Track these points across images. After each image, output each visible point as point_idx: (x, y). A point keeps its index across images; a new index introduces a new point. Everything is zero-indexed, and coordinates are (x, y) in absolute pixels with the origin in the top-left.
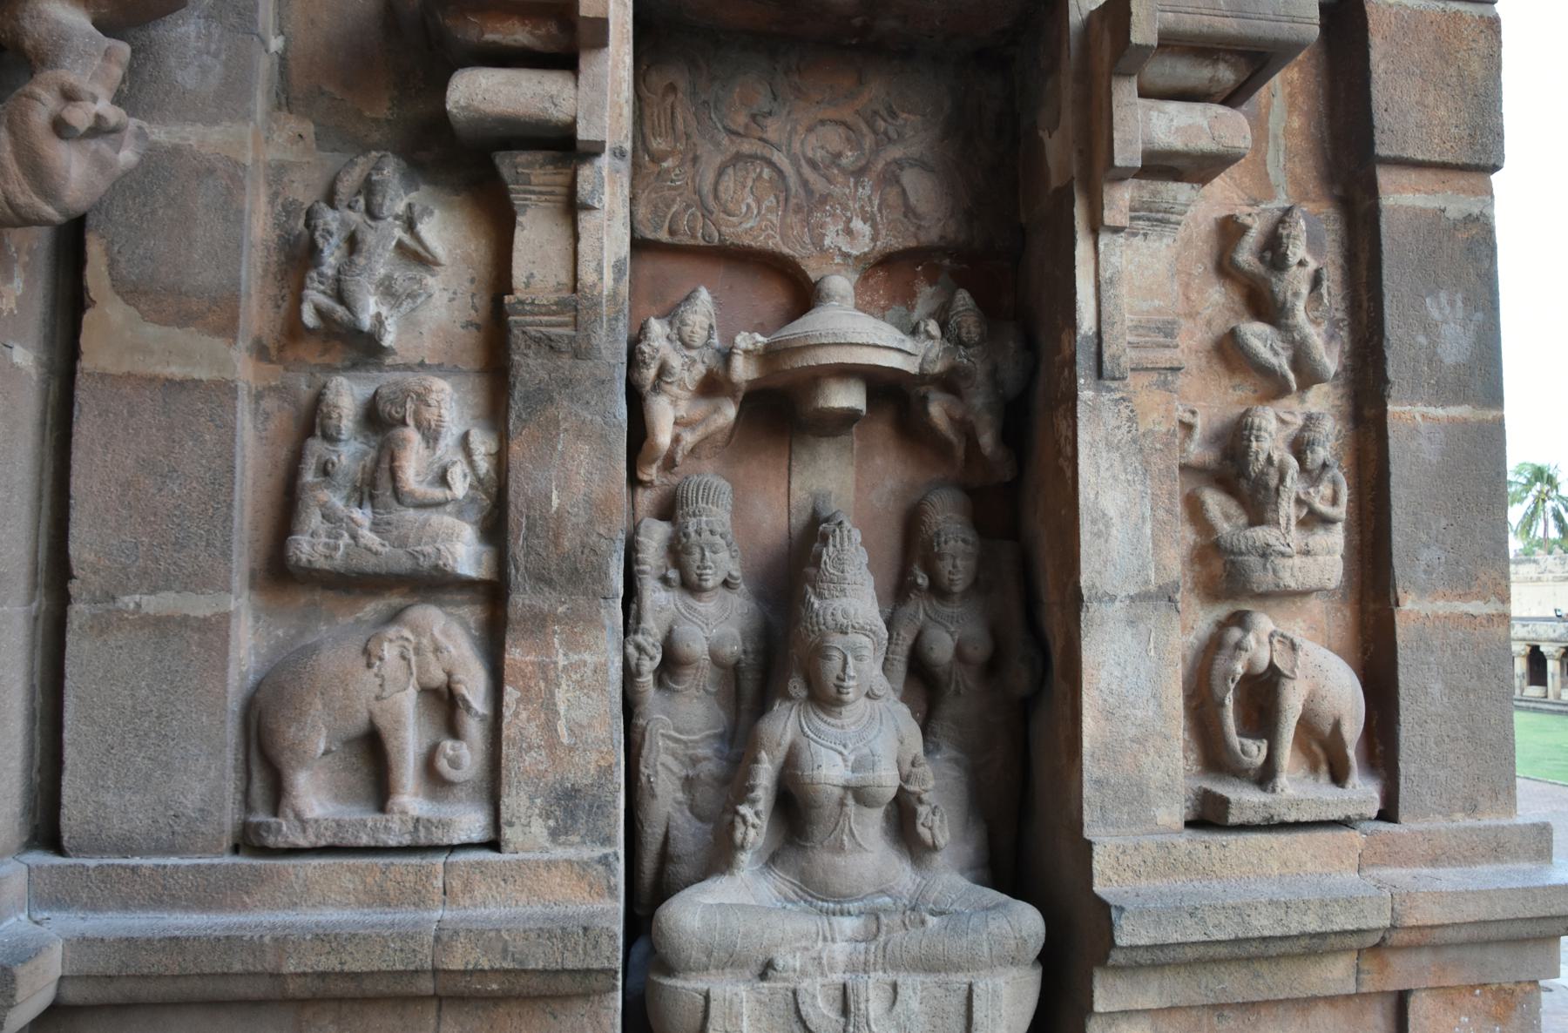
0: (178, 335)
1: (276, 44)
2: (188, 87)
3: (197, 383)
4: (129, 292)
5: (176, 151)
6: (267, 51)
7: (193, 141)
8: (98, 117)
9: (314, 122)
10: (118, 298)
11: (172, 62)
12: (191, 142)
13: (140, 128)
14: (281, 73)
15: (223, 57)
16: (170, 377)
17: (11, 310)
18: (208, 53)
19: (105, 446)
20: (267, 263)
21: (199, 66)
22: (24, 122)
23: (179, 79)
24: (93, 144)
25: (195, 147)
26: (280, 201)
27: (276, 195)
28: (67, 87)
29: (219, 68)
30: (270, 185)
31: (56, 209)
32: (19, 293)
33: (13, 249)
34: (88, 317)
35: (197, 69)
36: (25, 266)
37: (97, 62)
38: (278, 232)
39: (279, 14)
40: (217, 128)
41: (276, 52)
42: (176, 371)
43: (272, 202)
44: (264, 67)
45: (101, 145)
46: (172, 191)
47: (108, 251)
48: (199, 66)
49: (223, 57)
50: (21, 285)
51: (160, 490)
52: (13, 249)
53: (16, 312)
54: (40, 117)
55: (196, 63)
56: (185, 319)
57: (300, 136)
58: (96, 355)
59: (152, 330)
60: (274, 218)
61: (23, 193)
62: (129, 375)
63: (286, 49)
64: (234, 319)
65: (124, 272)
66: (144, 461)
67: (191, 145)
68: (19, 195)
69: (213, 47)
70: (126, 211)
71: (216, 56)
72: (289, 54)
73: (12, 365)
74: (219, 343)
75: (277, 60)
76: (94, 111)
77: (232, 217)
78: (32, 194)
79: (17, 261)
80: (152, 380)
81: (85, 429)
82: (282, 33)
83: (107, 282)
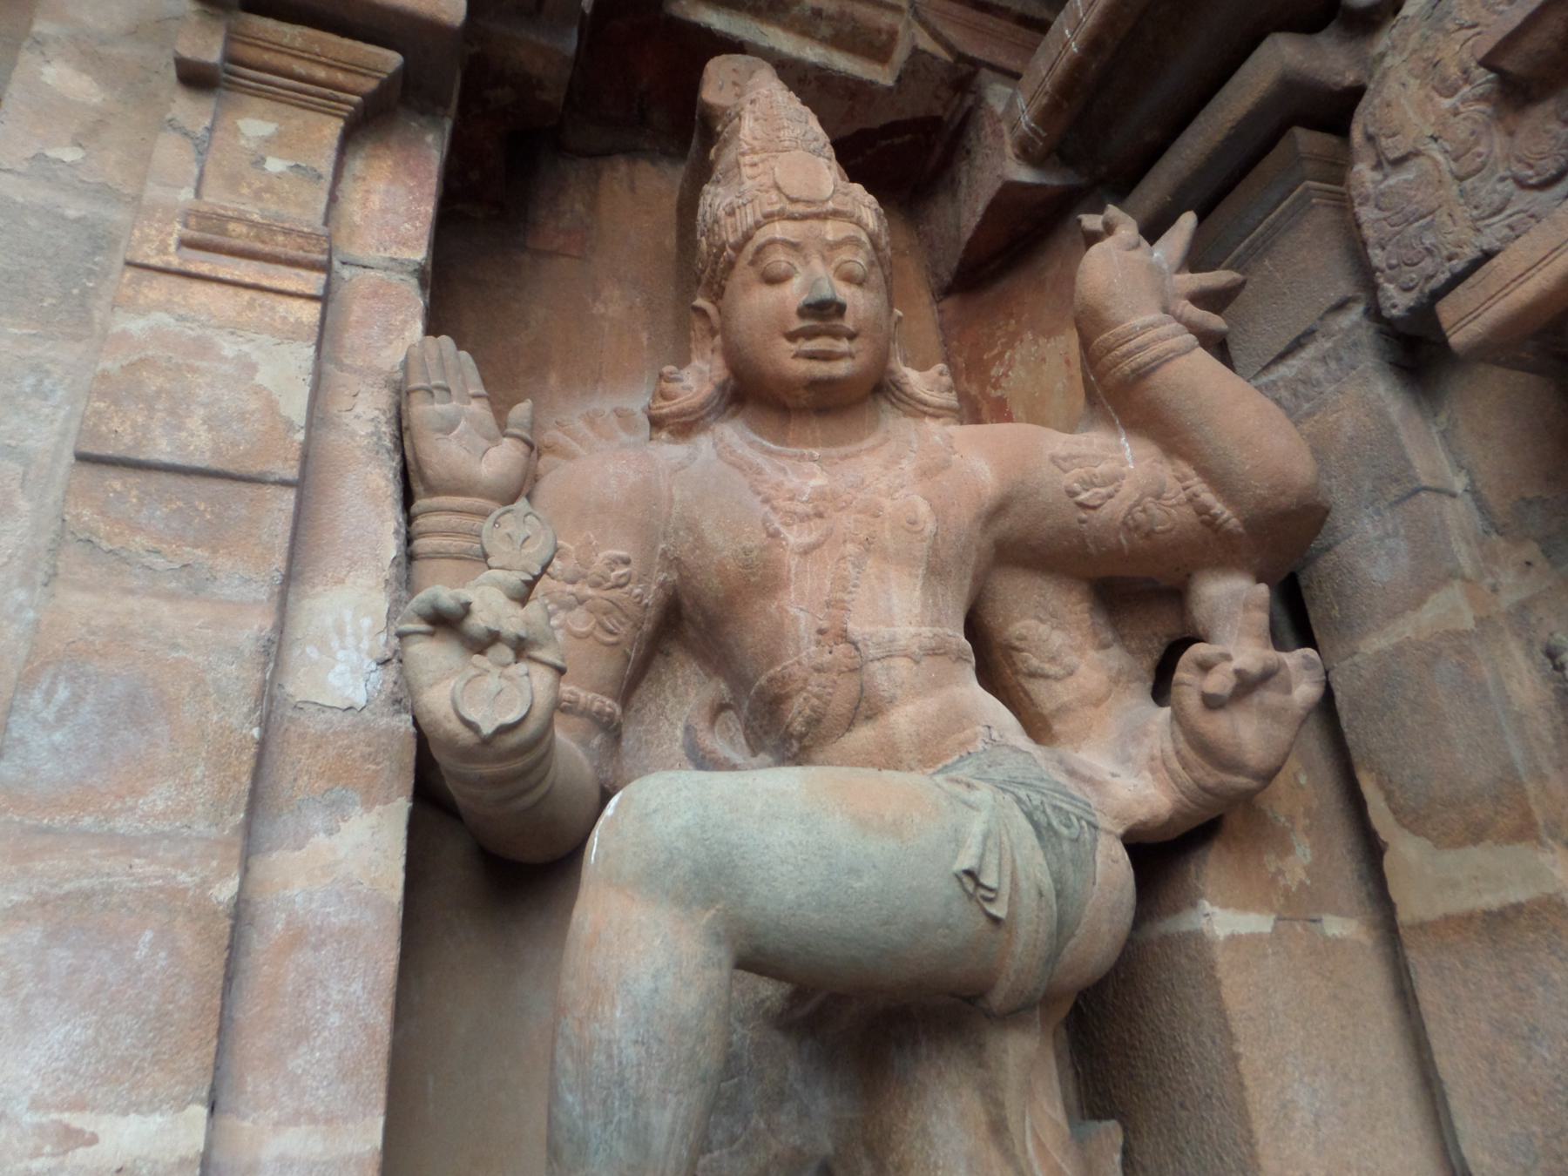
0: (1479, 855)
1: (1459, 483)
2: (1385, 580)
3: (1518, 908)
4: (1413, 819)
5: (1399, 650)
6: (1453, 495)
7: (1409, 633)
8: (1239, 673)
9: (1536, 540)
10: (1406, 832)
11: (1363, 564)
12: (1407, 635)
13: (1305, 657)
14: (1479, 508)
15: (1402, 531)
16: (1486, 908)
17: (1302, 883)
18: (1388, 535)
19: (1453, 1011)
20: (1555, 728)
21: (1387, 554)
22: (1182, 709)
23: (1375, 577)
24: (1256, 698)
25: (1413, 637)
26: (1538, 648)
27: (1530, 642)
28: (1200, 658)
29: (1403, 546)
30: (1519, 636)
31: (1247, 776)
32: (1309, 859)
33: (1283, 819)
34: (1389, 862)
35: (1385, 558)
36: (1307, 831)
37: (1240, 616)
38: (1552, 686)
39: (1449, 450)
40: (1426, 607)
41: (1466, 490)
42: (1491, 900)
43: (1529, 655)
44: (1458, 515)
45: (1269, 696)
46: (1411, 695)
47: (1381, 785)
48: (1387, 554)
49: (1402, 531)
50: (1308, 852)
51: (1529, 1058)
52: (1283, 819)
53: (1308, 882)
54: (1192, 702)
55: (1383, 552)
56: (1476, 834)
57: (1528, 564)
58: (1412, 905)
59: (1450, 857)
60: (1539, 671)
61: (1209, 775)
62: (1447, 918)
63: (1472, 482)
64: (1527, 814)
65: (1402, 802)
66: (1497, 1021)
67: (1408, 638)
68: (1206, 778)
69: (1390, 527)
70: (1380, 735)
71: (1396, 534)
72: (1479, 485)
73: (1327, 939)
74: (1522, 850)
75: (1468, 497)
76: (1231, 669)
77: (1477, 696)
78: (1216, 772)
79: (1292, 830)
80: (1470, 917)
81: (1429, 996)
82: (1463, 468)
83: (1390, 819)
